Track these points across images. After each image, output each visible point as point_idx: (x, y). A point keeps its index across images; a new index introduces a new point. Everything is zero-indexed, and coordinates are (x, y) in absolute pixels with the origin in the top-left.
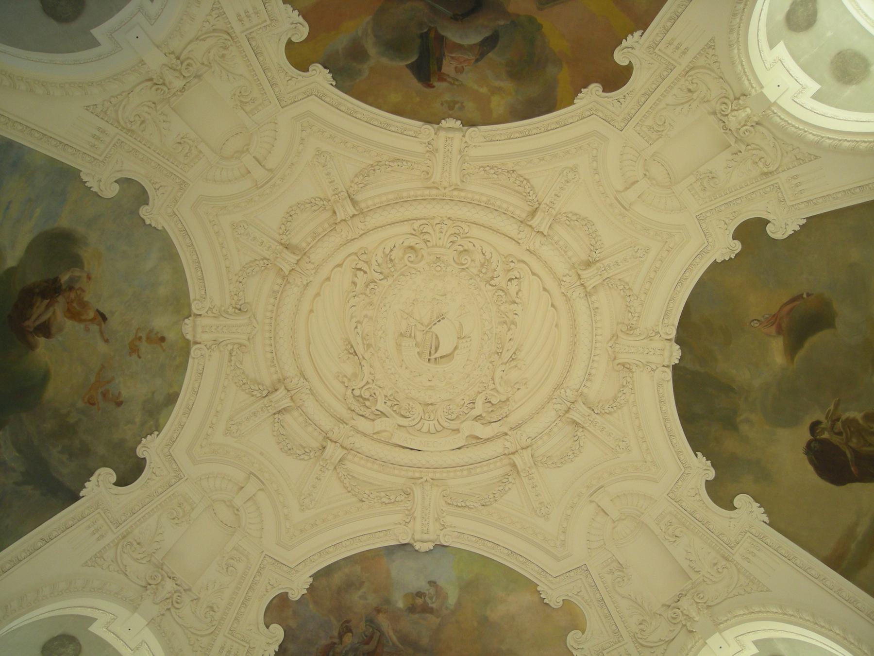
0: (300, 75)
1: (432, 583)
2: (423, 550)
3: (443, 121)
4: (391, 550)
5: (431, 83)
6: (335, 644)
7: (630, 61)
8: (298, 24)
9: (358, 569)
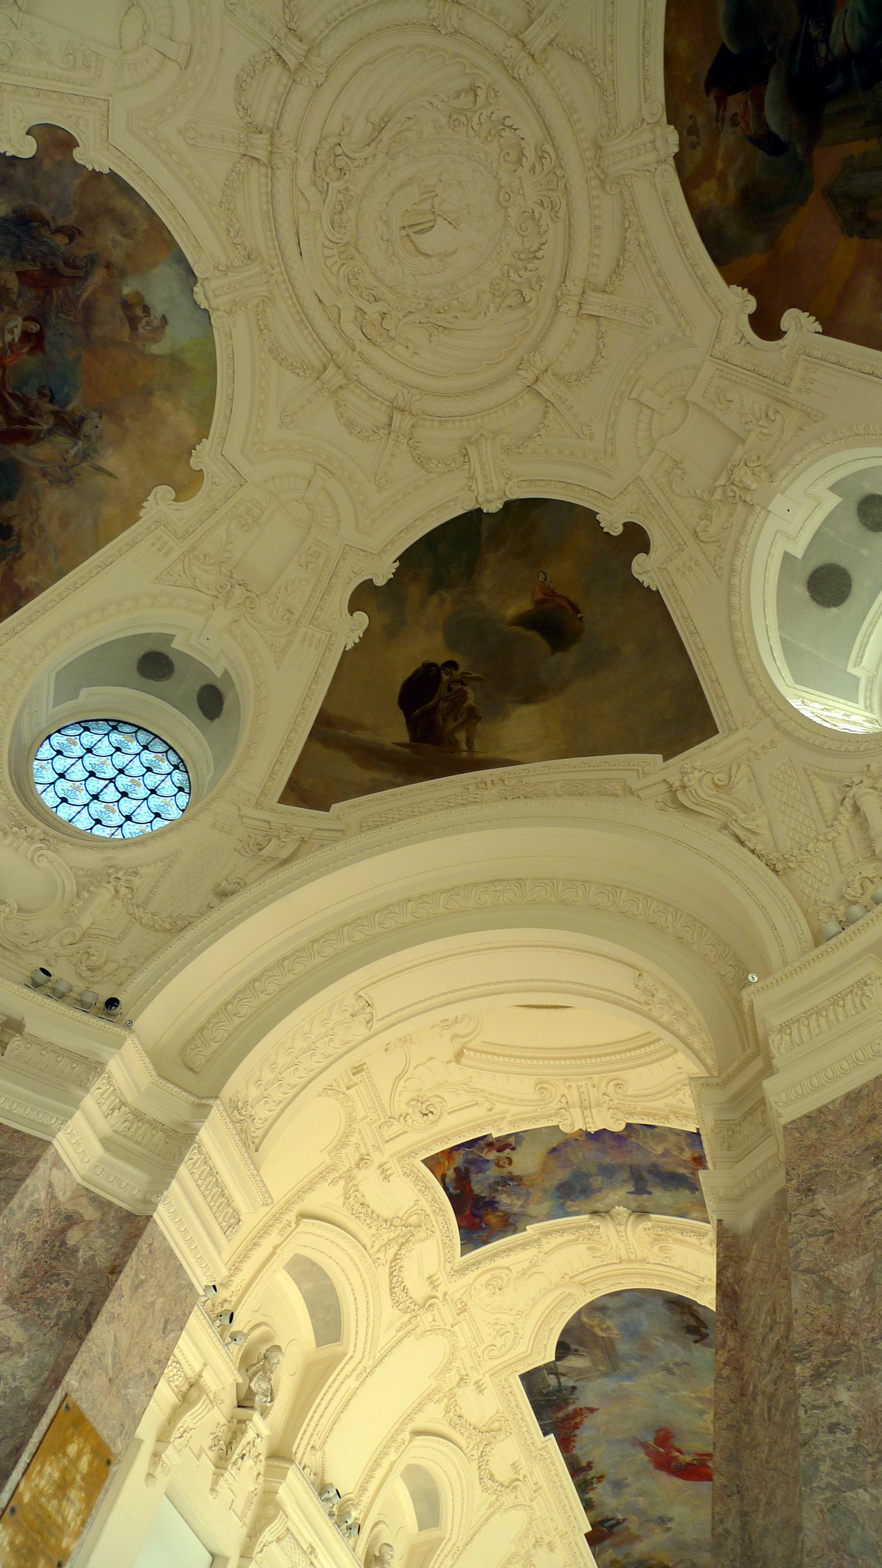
1: (164, 320)
2: (196, 297)
4: (181, 259)
6: (49, 226)
9: (143, 226)
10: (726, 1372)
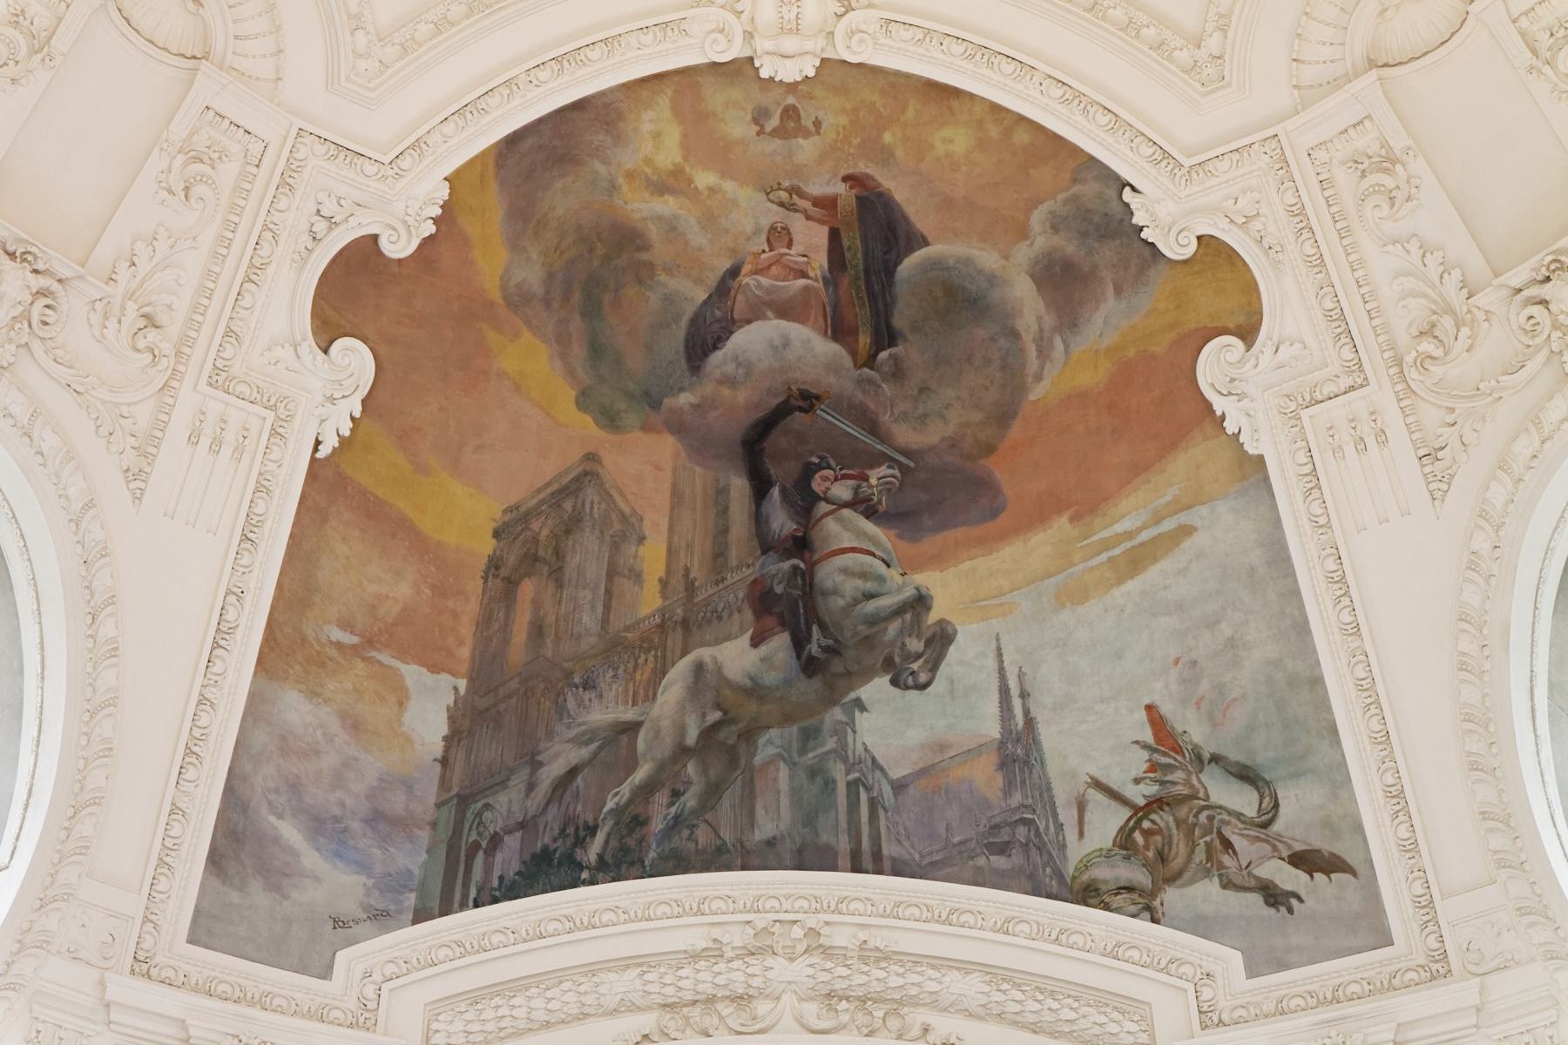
0: (1223, 230)
3: (811, 73)
5: (854, 191)
7: (326, 351)
8: (1225, 393)
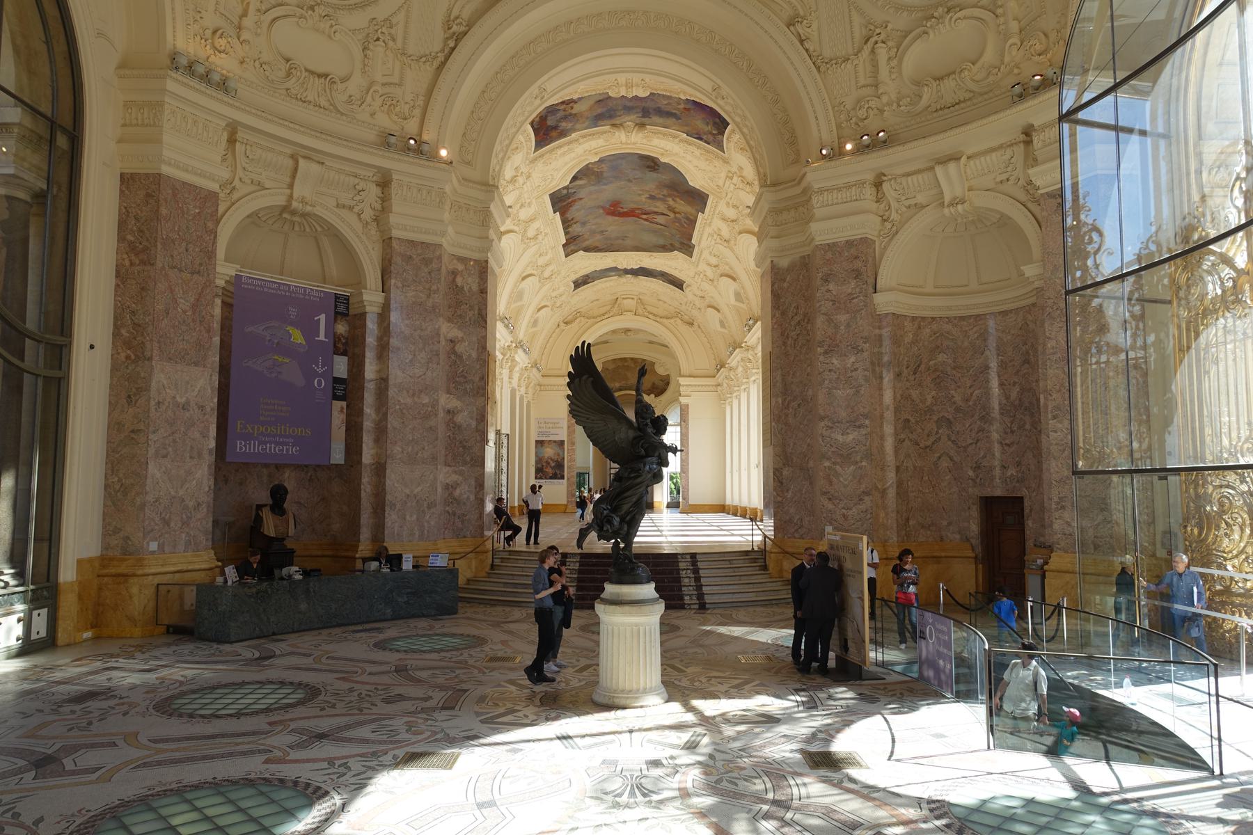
10: (776, 326)
